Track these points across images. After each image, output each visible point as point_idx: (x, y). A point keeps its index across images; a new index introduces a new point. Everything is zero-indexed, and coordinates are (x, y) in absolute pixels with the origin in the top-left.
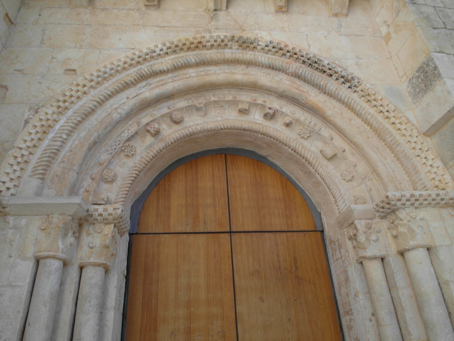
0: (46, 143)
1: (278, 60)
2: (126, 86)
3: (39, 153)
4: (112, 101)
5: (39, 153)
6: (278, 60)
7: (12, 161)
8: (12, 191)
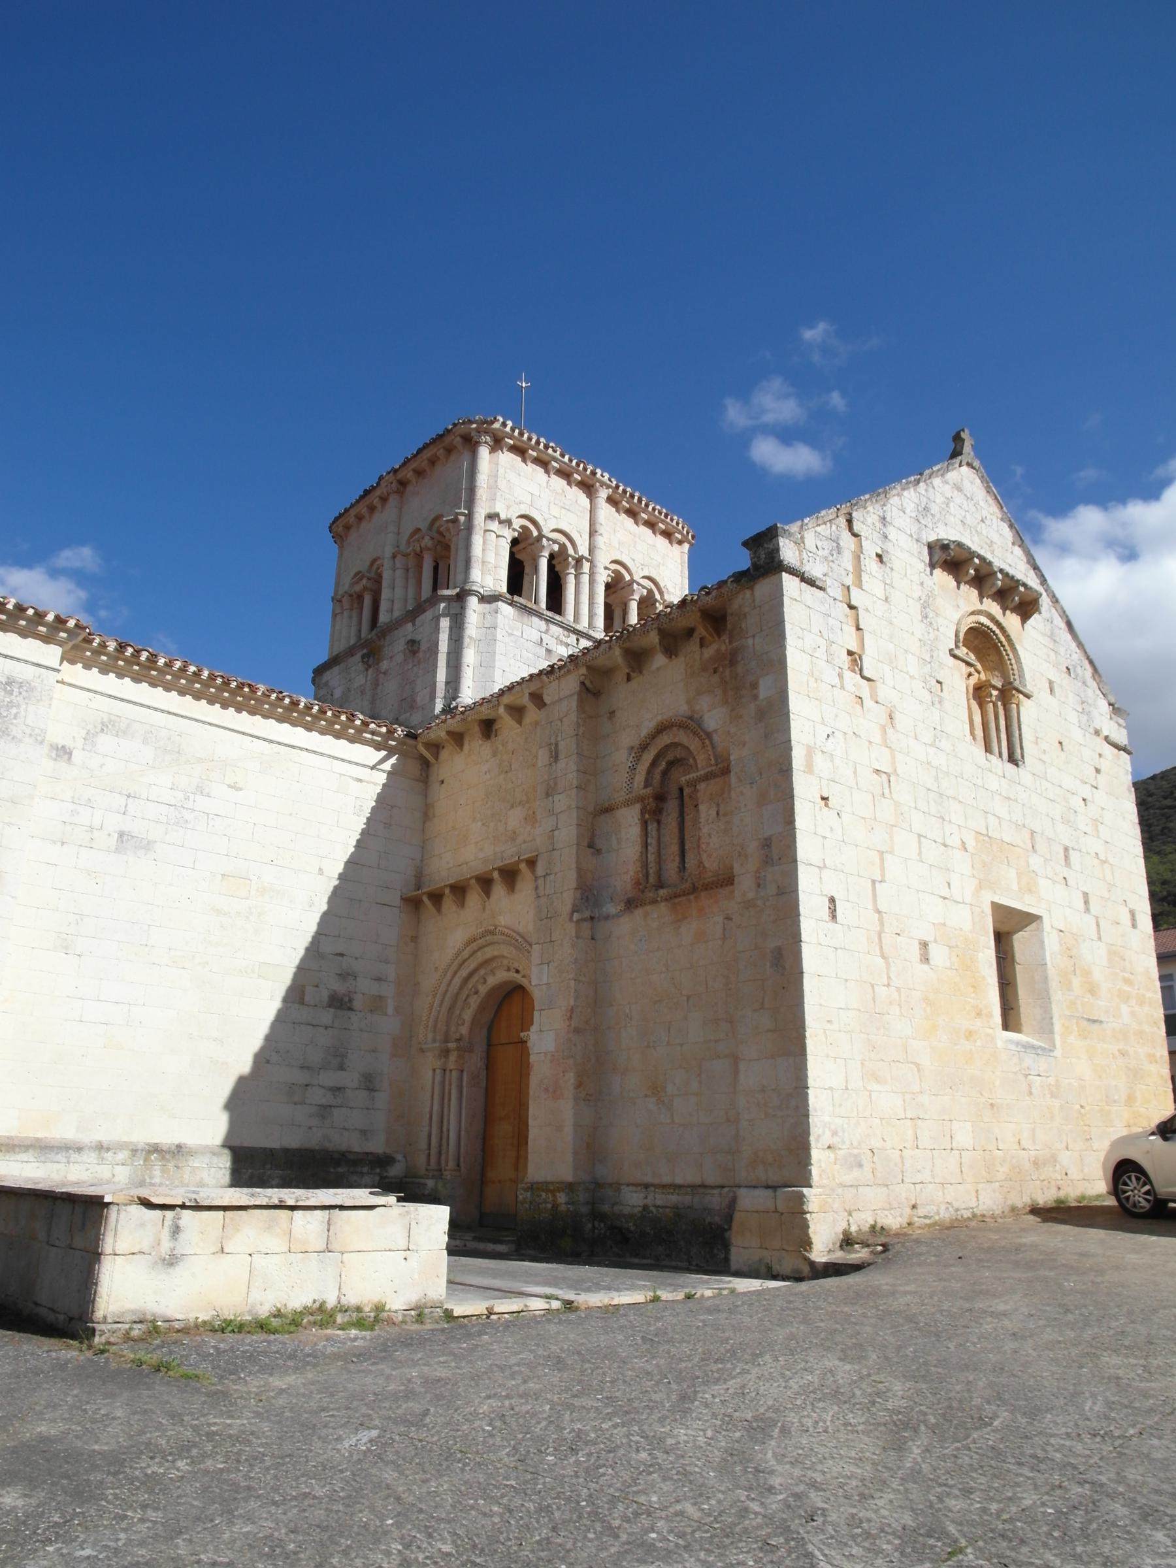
2: (456, 973)
3: (431, 1020)
5: (431, 1020)
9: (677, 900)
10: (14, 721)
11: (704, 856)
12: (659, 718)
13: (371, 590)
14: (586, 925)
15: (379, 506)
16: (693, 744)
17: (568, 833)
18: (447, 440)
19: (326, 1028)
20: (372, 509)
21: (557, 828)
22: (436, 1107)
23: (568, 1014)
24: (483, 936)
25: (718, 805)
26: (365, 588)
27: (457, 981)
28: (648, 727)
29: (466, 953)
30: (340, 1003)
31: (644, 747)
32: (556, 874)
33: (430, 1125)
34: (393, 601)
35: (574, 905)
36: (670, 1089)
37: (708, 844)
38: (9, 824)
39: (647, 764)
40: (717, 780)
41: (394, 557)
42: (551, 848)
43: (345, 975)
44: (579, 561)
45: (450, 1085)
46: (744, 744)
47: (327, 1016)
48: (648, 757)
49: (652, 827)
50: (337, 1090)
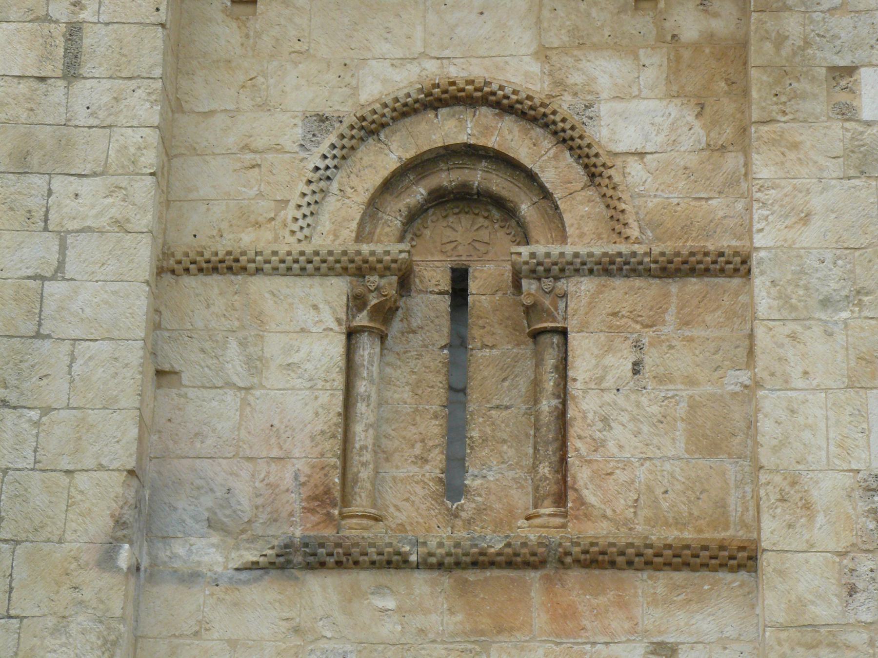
9: (472, 576)
21: (59, 272)
25: (638, 346)
32: (47, 410)
35: (119, 523)
37: (598, 445)
39: (375, 179)
40: (638, 282)
42: (29, 328)
46: (806, 219)
49: (367, 349)
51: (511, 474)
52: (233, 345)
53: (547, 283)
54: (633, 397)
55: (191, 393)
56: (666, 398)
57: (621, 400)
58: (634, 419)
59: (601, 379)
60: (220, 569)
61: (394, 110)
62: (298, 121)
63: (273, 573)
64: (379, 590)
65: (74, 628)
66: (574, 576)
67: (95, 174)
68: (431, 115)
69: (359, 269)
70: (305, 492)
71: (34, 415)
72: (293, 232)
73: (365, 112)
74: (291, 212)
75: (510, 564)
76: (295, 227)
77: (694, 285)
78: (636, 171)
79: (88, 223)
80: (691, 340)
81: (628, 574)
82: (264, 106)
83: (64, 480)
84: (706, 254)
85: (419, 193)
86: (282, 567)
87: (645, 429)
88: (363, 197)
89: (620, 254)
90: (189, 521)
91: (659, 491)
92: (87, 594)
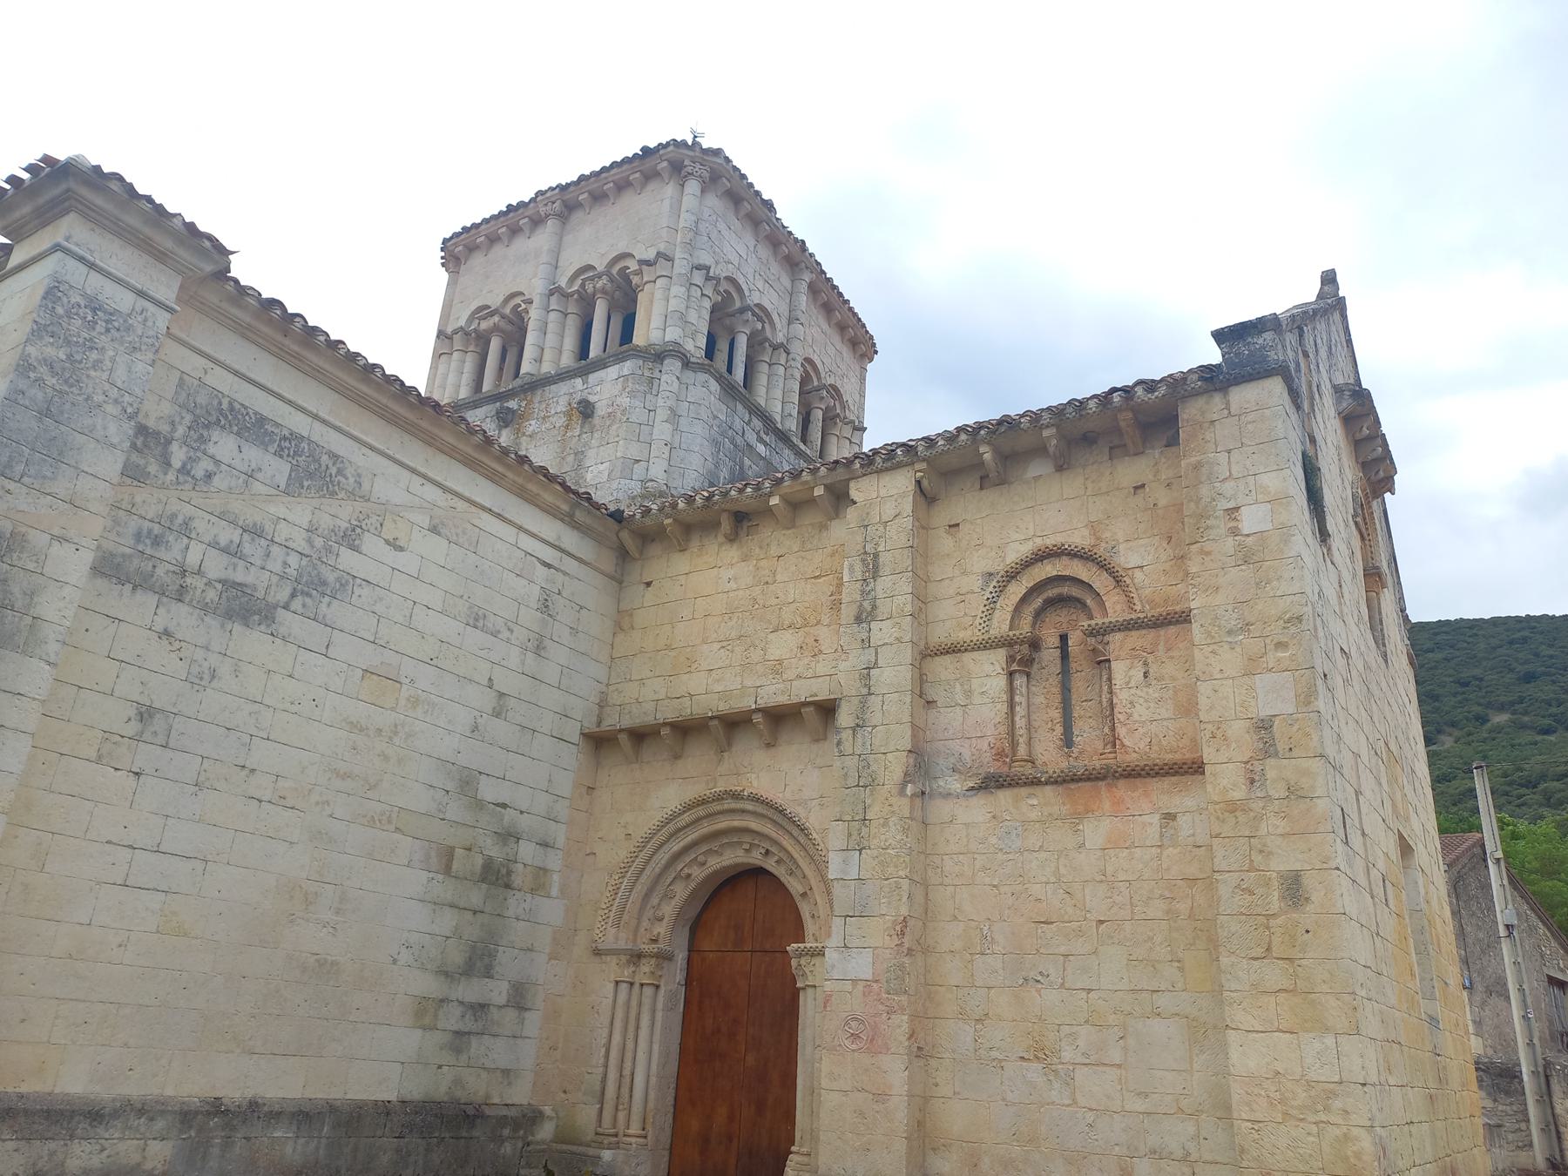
0: (618, 900)
1: (760, 809)
4: (655, 857)
6: (760, 809)
7: (600, 919)
8: (602, 939)
9: (1073, 786)
10: (92, 373)
11: (1121, 731)
12: (1039, 541)
13: (502, 331)
14: (918, 801)
15: (527, 232)
16: (1100, 582)
17: (894, 673)
18: (649, 163)
19: (475, 912)
20: (515, 231)
22: (617, 1038)
23: (898, 928)
24: (719, 798)
25: (1146, 664)
26: (496, 329)
27: (663, 857)
28: (1018, 551)
29: (687, 818)
30: (496, 876)
31: (1012, 575)
33: (606, 1066)
34: (543, 350)
36: (1067, 1055)
37: (1129, 716)
38: (62, 539)
39: (1016, 599)
40: (1144, 632)
41: (551, 293)
42: (865, 691)
43: (509, 836)
44: (775, 348)
45: (640, 1005)
47: (476, 896)
48: (1017, 590)
49: (1020, 681)
50: (480, 1009)
51: (1095, 733)
52: (958, 685)
53: (1100, 637)
54: (1145, 689)
55: (942, 710)
56: (1161, 689)
57: (1138, 692)
58: (1146, 701)
59: (1128, 683)
60: (958, 791)
61: (1021, 565)
62: (980, 578)
63: (982, 791)
64: (1030, 796)
65: (891, 824)
66: (1122, 783)
67: (888, 619)
68: (1040, 564)
69: (1009, 643)
70: (994, 751)
71: (870, 729)
72: (980, 630)
73: (1008, 568)
74: (978, 620)
75: (1089, 779)
76: (981, 627)
77: (1172, 630)
78: (1138, 575)
79: (886, 641)
80: (1172, 658)
81: (1148, 780)
82: (964, 573)
83: (883, 757)
84: (1176, 613)
85: (1039, 602)
86: (985, 788)
87: (1152, 705)
88: (1011, 609)
89: (1132, 619)
90: (945, 770)
91: (1161, 736)
92: (896, 808)
